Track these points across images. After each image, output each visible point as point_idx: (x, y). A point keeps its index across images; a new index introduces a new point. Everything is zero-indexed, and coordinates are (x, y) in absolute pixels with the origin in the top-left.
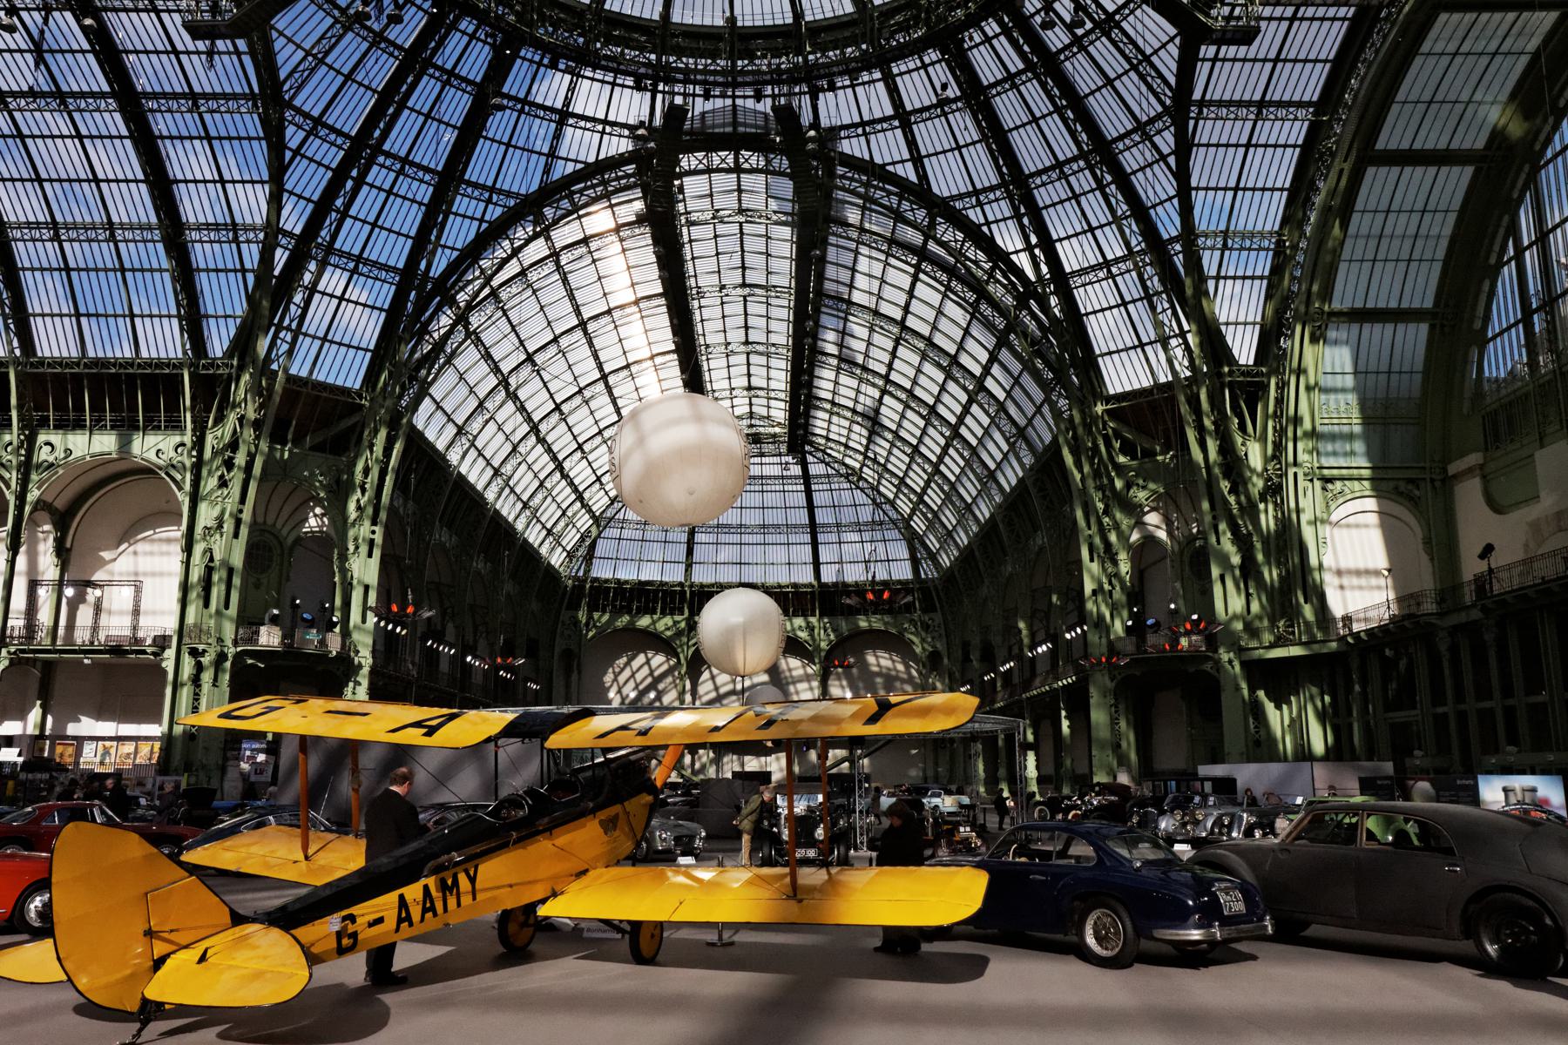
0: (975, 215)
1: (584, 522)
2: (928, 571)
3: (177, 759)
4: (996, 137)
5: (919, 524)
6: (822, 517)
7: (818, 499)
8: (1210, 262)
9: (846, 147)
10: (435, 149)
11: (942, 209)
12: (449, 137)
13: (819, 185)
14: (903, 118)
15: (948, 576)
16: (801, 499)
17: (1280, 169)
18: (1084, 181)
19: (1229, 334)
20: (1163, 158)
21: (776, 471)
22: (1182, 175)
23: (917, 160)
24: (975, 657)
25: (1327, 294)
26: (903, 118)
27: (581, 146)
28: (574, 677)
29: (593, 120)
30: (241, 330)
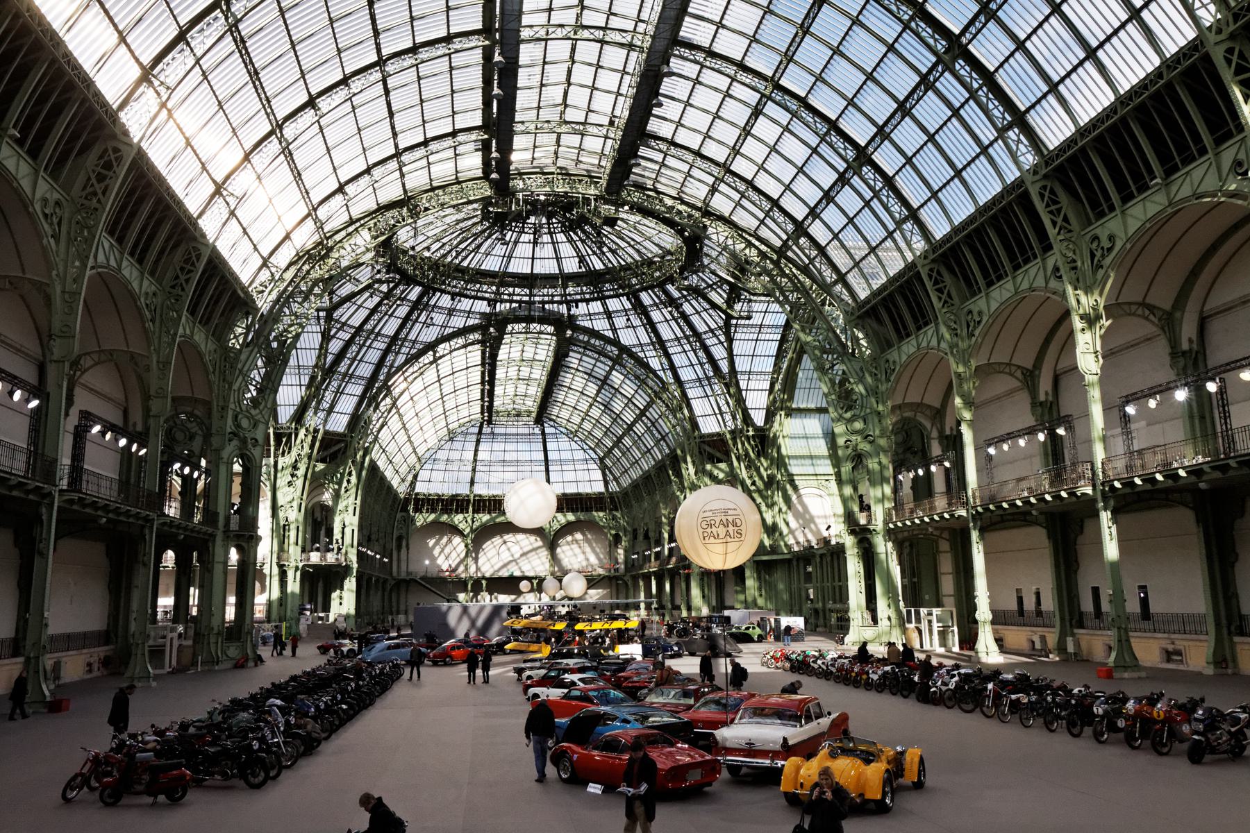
0: (641, 355)
1: (412, 459)
2: (614, 487)
3: (274, 615)
4: (651, 326)
5: (608, 462)
6: (551, 456)
7: (549, 446)
8: (743, 385)
9: (581, 323)
10: (391, 328)
11: (624, 349)
12: (400, 321)
13: (569, 337)
14: (608, 314)
15: (625, 493)
16: (541, 446)
17: (773, 348)
18: (687, 347)
19: (752, 413)
20: (721, 343)
21: (526, 431)
22: (730, 351)
23: (614, 330)
24: (641, 537)
25: (791, 398)
26: (608, 314)
27: (458, 322)
28: (404, 551)
29: (464, 311)
30: (296, 412)
